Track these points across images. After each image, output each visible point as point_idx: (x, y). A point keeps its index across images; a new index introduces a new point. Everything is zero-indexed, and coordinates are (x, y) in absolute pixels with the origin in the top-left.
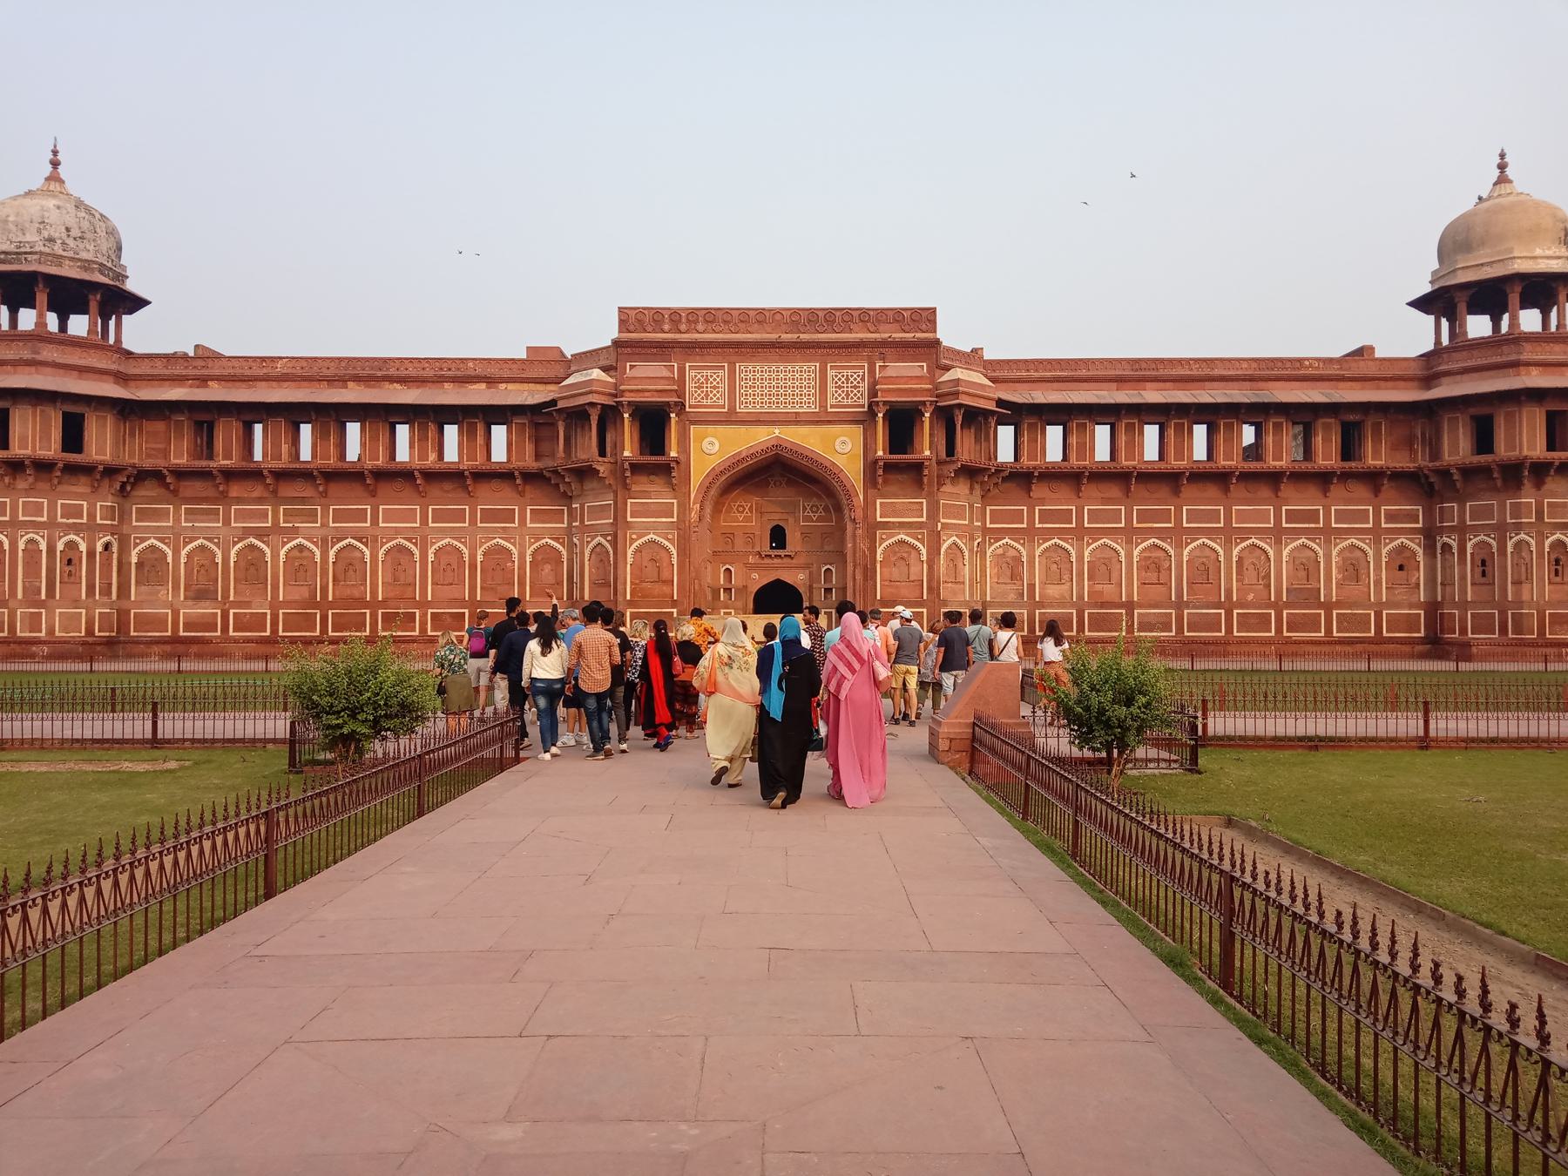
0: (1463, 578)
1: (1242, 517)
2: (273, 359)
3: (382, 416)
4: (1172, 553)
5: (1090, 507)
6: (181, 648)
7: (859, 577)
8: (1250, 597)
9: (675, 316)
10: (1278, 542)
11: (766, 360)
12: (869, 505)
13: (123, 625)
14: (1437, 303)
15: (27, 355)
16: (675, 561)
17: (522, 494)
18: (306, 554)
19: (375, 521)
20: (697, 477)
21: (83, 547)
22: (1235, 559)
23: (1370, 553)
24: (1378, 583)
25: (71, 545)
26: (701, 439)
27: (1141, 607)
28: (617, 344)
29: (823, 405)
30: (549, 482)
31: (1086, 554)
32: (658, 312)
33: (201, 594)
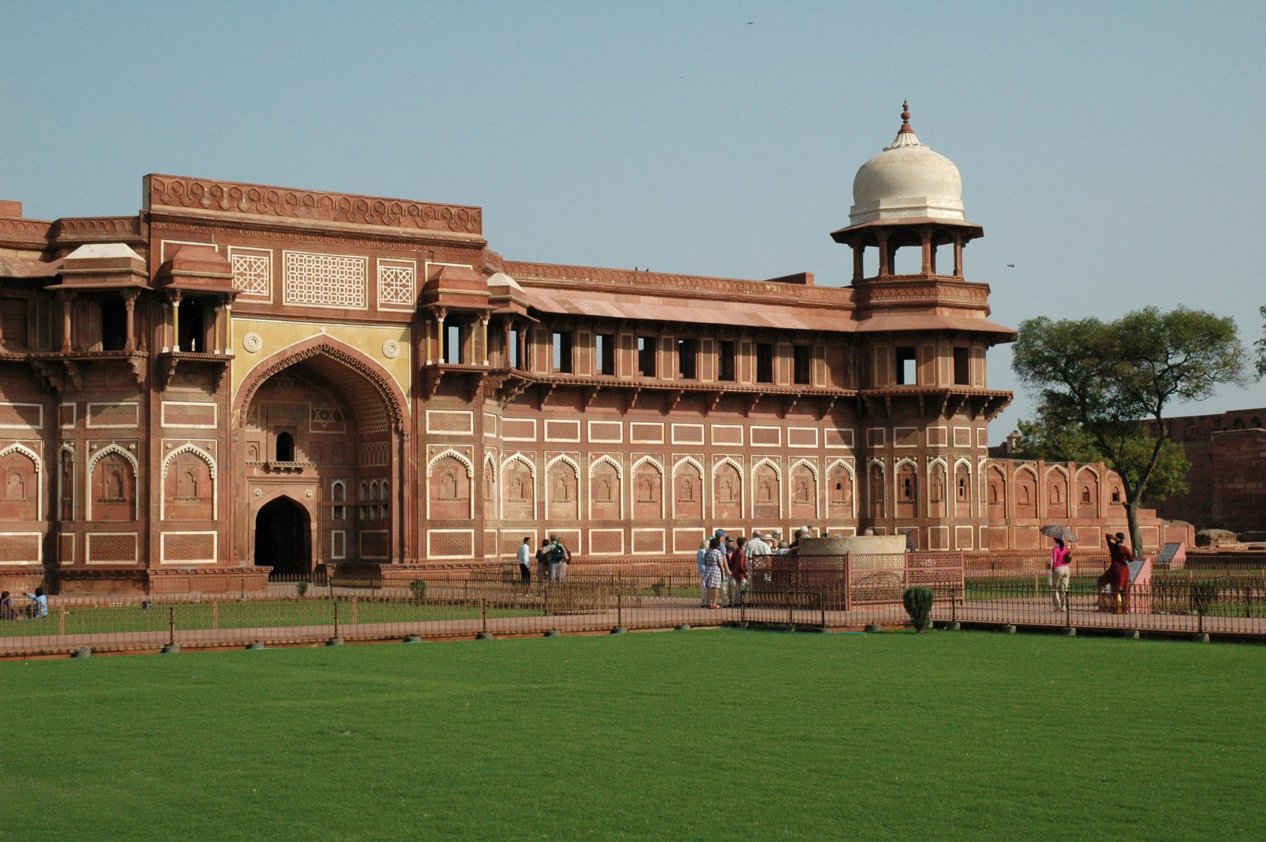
1: (721, 435)
4: (662, 470)
8: (725, 515)
9: (216, 192)
10: (748, 461)
11: (314, 249)
20: (238, 376)
22: (713, 477)
24: (823, 501)
26: (242, 333)
27: (638, 524)
28: (149, 217)
29: (373, 306)
31: (590, 471)
32: (198, 184)
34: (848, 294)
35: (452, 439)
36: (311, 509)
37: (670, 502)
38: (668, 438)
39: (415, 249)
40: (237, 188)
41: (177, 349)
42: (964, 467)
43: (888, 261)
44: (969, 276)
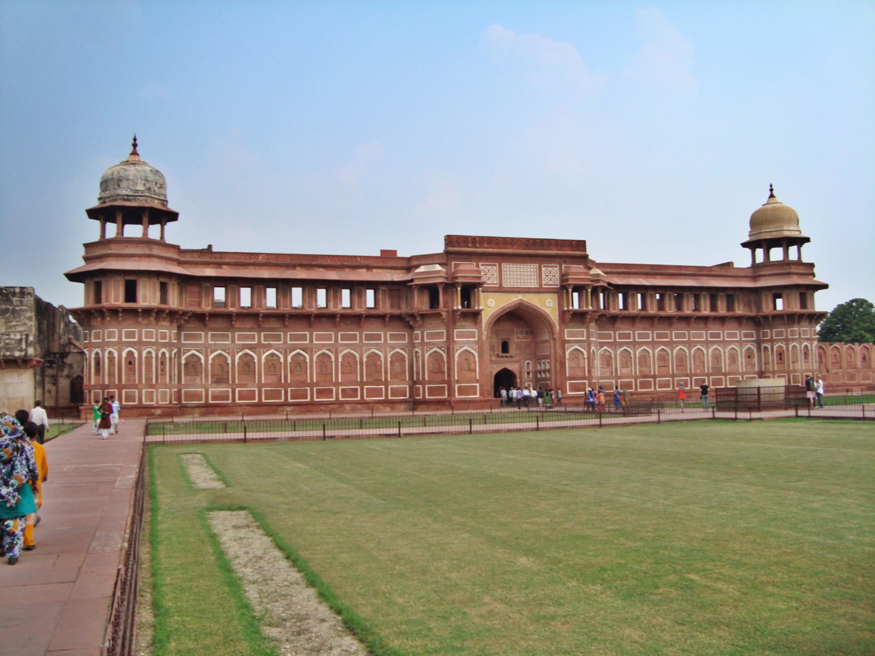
0: (773, 361)
1: (695, 336)
2: (258, 254)
3: (310, 286)
4: (669, 351)
5: (636, 333)
6: (210, 410)
7: (558, 366)
8: (698, 371)
12: (562, 332)
13: (179, 399)
14: (751, 245)
15: (146, 251)
16: (477, 359)
17: (385, 326)
18: (275, 358)
19: (311, 340)
20: (486, 317)
21: (167, 355)
23: (739, 350)
25: (164, 354)
26: (486, 299)
28: (447, 253)
29: (541, 285)
30: (406, 322)
33: (220, 379)
34: (750, 271)
35: (577, 341)
36: (517, 373)
37: (672, 367)
38: (671, 338)
39: (558, 260)
40: (482, 238)
41: (460, 307)
42: (806, 347)
43: (767, 255)
44: (805, 260)
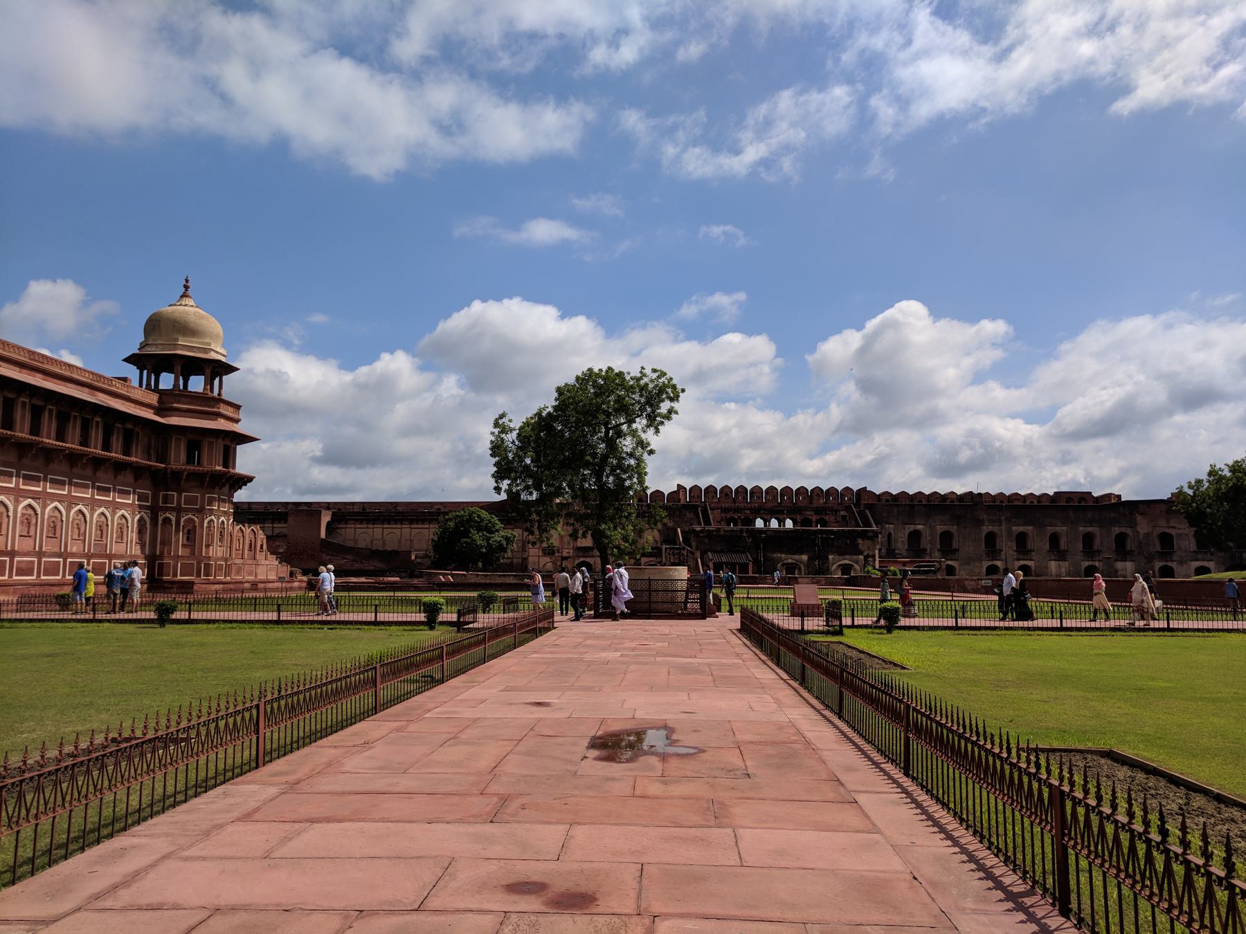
8: (74, 550)
